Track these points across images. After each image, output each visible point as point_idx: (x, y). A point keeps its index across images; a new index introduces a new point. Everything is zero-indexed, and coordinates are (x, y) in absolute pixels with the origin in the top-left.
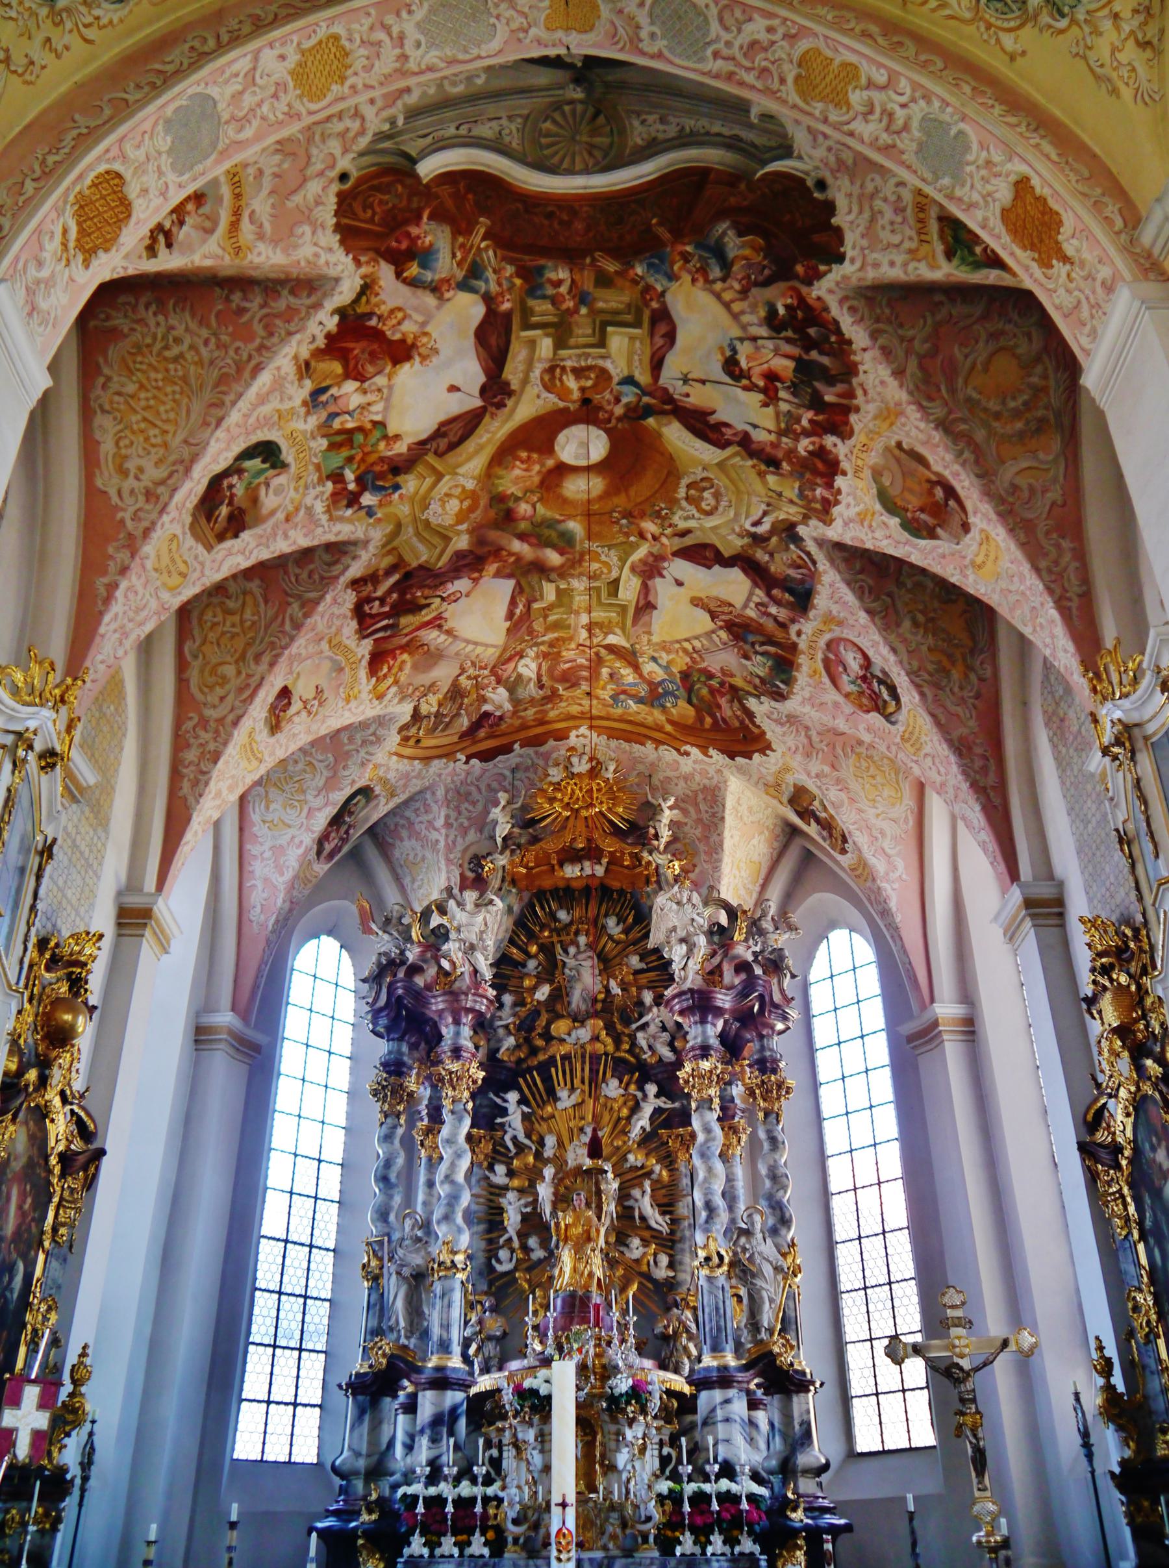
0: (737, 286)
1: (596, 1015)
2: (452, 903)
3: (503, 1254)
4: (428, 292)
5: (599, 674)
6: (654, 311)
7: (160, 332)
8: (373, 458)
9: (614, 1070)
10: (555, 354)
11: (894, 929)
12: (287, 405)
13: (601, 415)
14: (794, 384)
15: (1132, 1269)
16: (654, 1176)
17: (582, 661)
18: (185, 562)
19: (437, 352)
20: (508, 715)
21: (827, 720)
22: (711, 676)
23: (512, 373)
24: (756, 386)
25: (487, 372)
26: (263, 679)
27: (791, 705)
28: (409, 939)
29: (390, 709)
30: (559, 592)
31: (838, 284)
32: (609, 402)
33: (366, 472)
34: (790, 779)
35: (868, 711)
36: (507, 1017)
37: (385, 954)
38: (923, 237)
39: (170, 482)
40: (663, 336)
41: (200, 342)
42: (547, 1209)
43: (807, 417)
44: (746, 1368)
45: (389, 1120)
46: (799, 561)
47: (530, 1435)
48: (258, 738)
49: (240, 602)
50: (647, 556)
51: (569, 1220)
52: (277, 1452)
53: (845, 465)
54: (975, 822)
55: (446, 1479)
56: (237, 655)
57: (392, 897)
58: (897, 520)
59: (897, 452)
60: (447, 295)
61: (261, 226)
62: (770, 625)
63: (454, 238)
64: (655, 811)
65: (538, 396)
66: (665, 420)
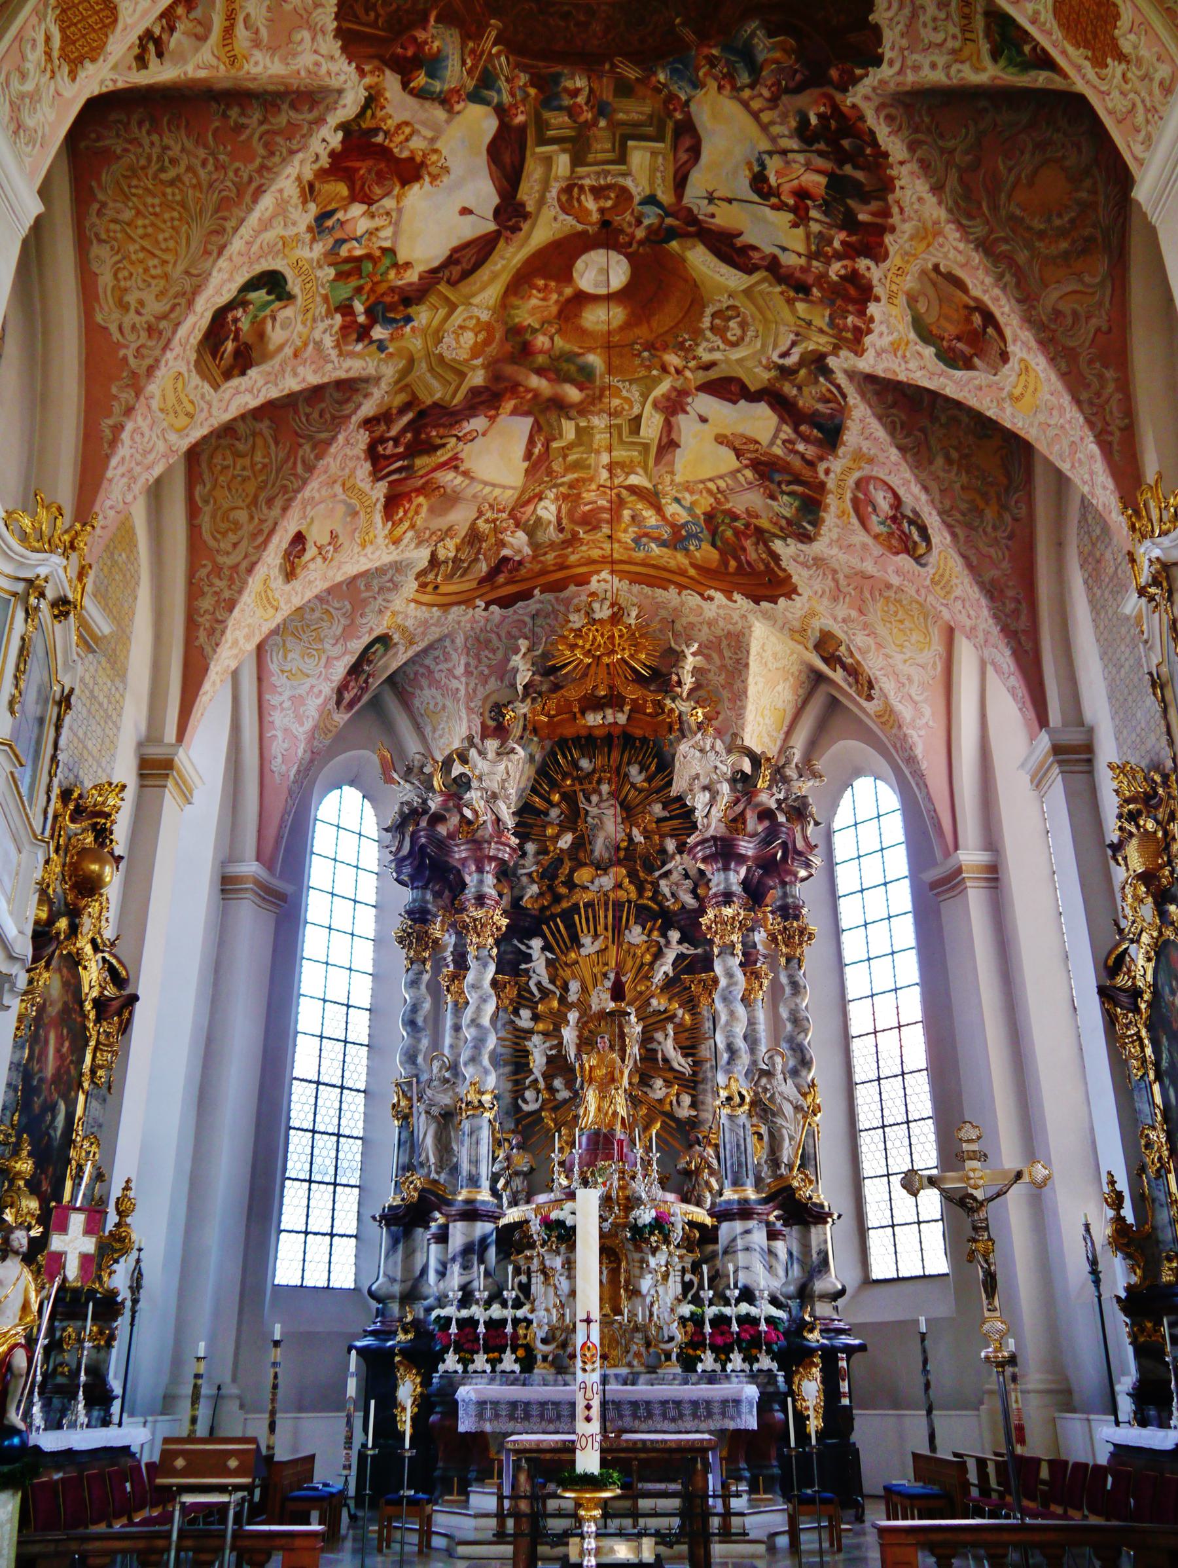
0: (766, 93)
1: (619, 863)
2: (473, 752)
3: (529, 1094)
4: (437, 105)
5: (619, 518)
6: (677, 122)
7: (156, 151)
8: (383, 288)
9: (637, 917)
10: (572, 171)
11: (919, 775)
12: (291, 231)
13: (622, 239)
14: (826, 203)
15: (1146, 1108)
16: (677, 1020)
17: (603, 503)
18: (192, 402)
19: (446, 169)
20: (528, 559)
21: (855, 562)
22: (735, 517)
23: (527, 193)
24: (786, 205)
25: (501, 193)
26: (276, 524)
27: (819, 547)
28: (430, 788)
29: (407, 555)
30: (579, 430)
31: (874, 89)
32: (630, 224)
33: (377, 303)
34: (817, 624)
35: (897, 553)
36: (530, 866)
37: (408, 803)
38: (968, 35)
39: (172, 316)
40: (687, 150)
41: (197, 163)
42: (572, 1052)
43: (839, 239)
44: (765, 1201)
45: (415, 966)
46: (828, 395)
47: (557, 1262)
48: (273, 586)
49: (250, 442)
50: (669, 391)
51: (593, 1062)
52: (317, 1278)
53: (878, 290)
54: (1005, 666)
55: (477, 1303)
56: (248, 500)
57: (413, 747)
58: (932, 350)
59: (933, 275)
60: (457, 107)
61: (257, 32)
62: (797, 463)
63: (463, 45)
64: (679, 657)
65: (555, 219)
66: (689, 242)
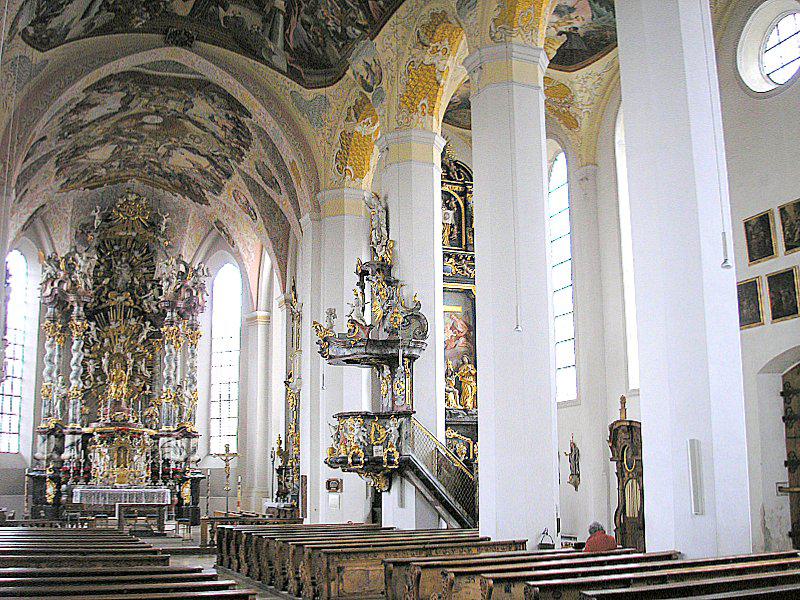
1: (127, 290)
28: (58, 267)
42: (106, 370)
47: (106, 450)
